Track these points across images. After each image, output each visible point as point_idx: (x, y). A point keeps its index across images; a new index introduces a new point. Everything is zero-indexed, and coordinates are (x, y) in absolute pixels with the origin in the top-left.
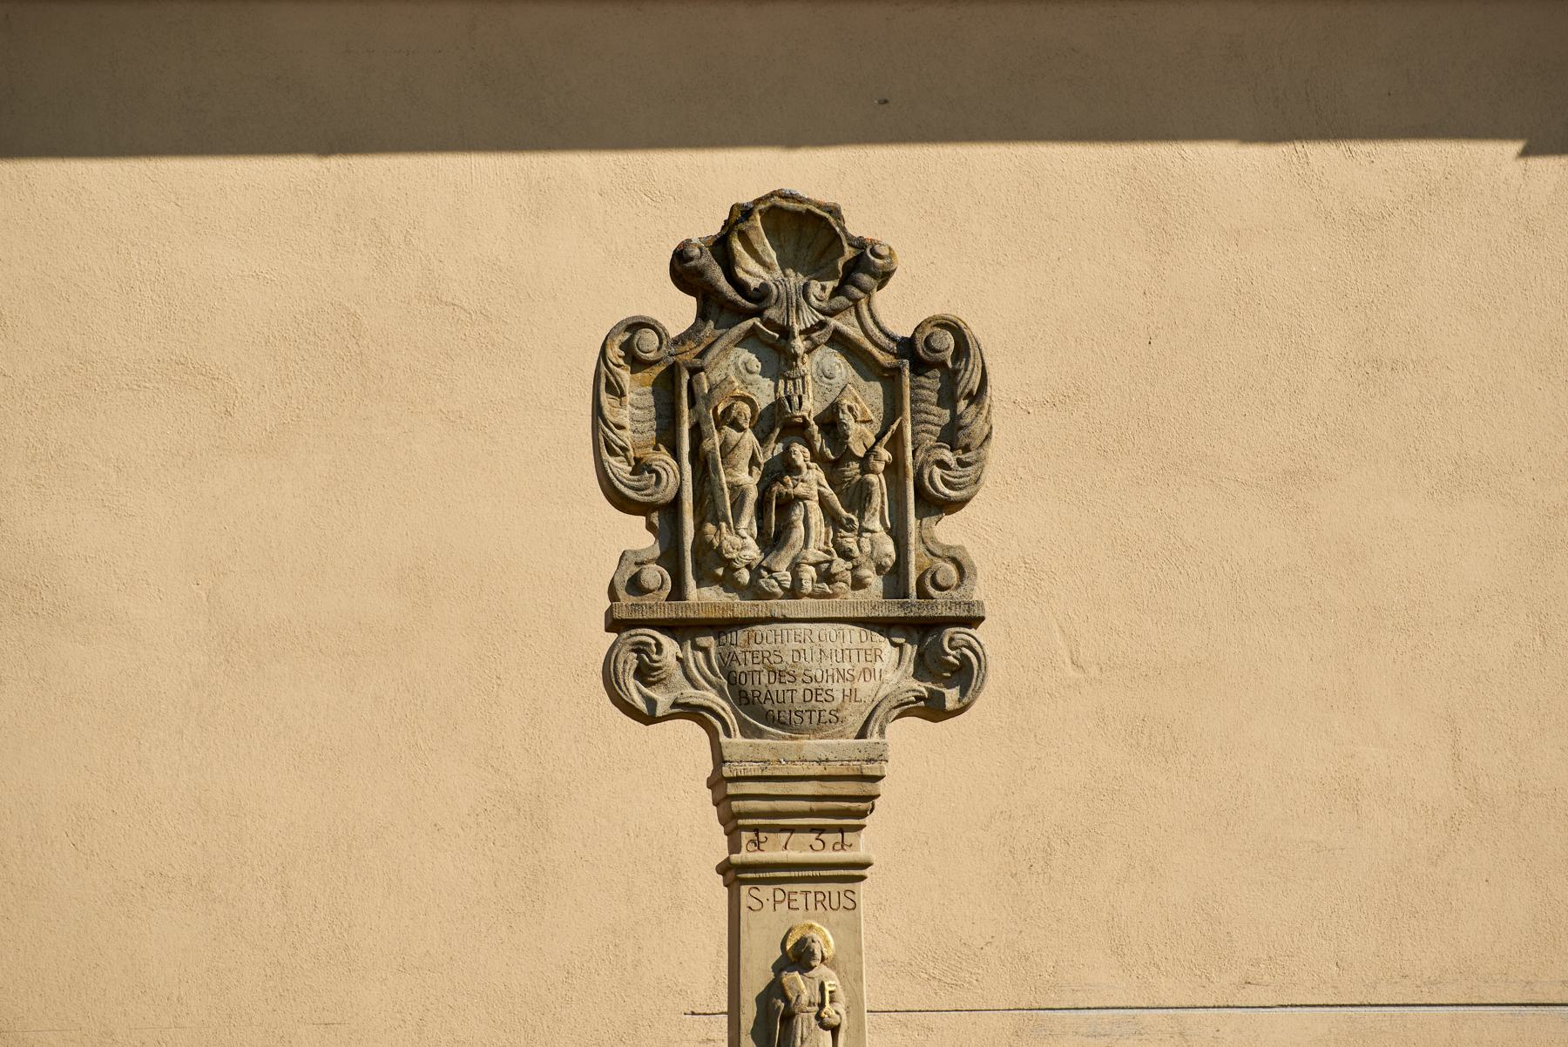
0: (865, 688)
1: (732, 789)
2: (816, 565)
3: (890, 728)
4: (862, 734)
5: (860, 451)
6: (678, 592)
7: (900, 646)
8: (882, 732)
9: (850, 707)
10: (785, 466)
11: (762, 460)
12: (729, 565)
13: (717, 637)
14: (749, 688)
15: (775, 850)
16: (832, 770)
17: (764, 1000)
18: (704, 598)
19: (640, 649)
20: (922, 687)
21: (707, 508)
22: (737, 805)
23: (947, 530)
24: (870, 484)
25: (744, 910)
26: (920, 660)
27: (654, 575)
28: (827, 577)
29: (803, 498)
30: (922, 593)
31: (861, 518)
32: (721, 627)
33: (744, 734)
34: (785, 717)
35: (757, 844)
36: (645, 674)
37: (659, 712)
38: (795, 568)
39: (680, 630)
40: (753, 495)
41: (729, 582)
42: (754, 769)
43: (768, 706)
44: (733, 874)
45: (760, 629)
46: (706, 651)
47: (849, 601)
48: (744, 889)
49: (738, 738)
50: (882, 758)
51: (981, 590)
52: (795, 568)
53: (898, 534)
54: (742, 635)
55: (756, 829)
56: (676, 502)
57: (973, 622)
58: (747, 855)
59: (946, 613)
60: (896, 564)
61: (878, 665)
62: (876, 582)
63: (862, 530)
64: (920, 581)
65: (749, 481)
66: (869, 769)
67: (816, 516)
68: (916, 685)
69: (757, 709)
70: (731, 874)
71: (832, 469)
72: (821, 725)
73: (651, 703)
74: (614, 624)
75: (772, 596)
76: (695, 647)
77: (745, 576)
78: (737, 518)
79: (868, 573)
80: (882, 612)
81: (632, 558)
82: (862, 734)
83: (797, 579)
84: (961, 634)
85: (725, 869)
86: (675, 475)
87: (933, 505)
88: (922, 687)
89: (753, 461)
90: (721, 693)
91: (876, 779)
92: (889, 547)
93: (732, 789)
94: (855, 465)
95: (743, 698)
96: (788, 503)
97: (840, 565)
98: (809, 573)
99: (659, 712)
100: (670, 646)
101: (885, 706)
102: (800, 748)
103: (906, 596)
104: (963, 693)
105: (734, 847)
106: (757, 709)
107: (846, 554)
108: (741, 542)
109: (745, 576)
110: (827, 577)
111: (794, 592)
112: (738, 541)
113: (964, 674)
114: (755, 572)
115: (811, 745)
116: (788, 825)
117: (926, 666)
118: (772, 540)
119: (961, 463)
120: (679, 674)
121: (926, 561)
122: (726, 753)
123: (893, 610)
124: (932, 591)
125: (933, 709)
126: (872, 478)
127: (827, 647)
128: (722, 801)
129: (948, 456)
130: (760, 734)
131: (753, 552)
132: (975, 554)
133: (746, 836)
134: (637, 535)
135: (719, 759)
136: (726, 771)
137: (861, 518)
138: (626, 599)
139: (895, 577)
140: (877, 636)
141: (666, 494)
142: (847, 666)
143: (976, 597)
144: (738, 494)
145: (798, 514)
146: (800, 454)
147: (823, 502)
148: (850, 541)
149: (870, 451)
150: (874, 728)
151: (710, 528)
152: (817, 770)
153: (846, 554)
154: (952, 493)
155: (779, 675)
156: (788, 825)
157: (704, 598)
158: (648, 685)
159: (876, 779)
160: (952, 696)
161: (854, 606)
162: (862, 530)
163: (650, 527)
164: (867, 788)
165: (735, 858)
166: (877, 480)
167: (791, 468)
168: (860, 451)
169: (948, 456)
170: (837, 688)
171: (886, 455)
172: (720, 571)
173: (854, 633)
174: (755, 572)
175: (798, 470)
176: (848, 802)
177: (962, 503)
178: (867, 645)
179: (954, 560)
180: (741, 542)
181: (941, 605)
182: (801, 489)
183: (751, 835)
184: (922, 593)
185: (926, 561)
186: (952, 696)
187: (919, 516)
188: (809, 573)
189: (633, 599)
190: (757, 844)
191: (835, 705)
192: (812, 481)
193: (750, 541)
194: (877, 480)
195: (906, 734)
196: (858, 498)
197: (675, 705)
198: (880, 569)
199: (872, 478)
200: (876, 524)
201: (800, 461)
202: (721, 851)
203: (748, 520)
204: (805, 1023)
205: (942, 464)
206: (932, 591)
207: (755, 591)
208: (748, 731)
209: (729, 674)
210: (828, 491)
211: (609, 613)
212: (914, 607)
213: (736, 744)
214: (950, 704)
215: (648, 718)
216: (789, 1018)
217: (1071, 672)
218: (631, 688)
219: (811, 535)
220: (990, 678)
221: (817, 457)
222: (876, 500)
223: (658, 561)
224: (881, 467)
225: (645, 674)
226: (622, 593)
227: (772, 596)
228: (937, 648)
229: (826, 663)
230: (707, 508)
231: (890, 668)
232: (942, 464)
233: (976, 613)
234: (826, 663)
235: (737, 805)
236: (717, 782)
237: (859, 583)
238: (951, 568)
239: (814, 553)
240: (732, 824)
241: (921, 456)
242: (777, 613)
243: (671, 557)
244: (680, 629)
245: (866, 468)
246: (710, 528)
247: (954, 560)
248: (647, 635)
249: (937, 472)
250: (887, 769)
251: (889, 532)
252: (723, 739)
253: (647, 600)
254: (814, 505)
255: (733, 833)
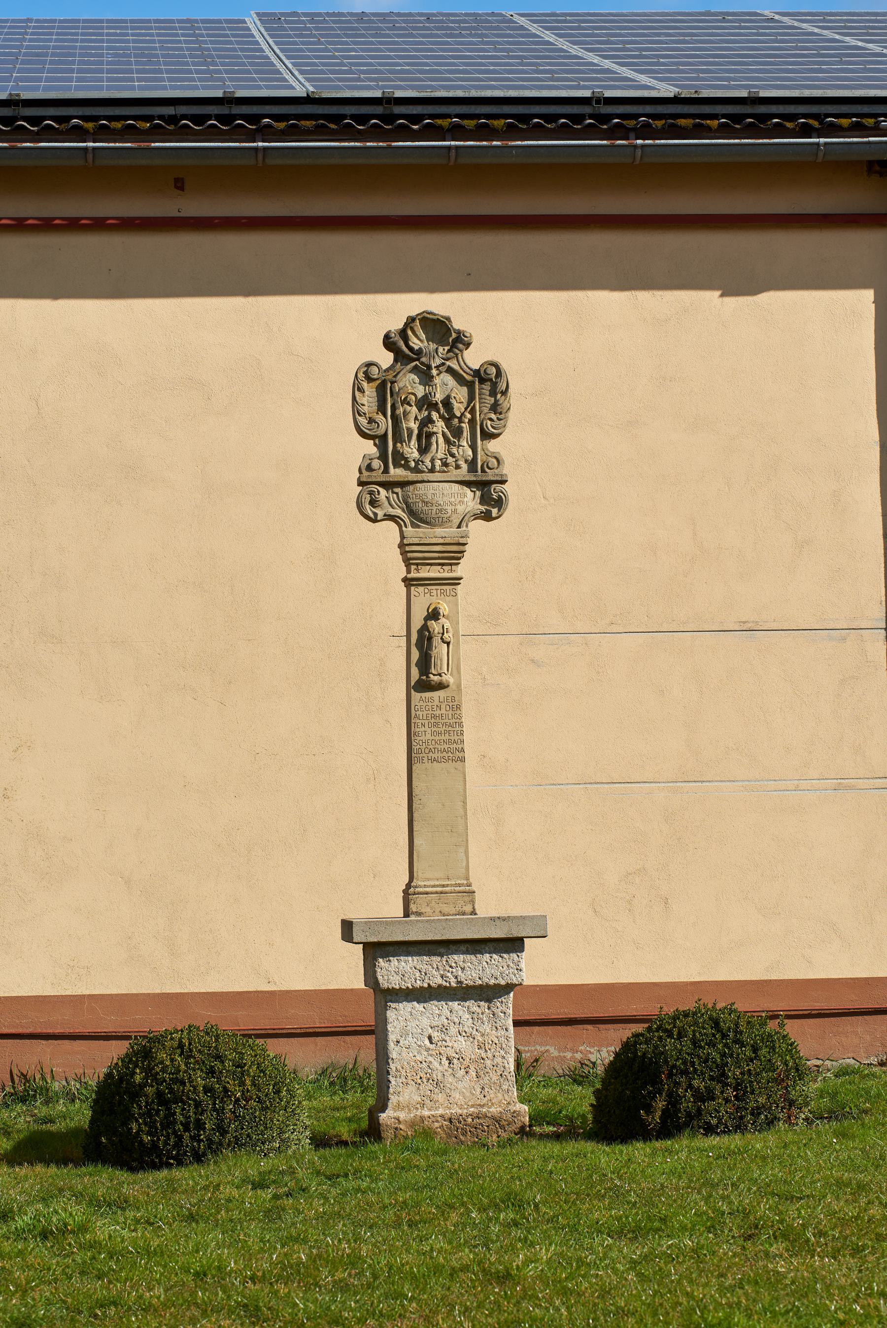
0: (461, 509)
1: (407, 549)
2: (441, 460)
3: (470, 524)
4: (459, 527)
5: (458, 415)
6: (386, 471)
7: (474, 492)
8: (467, 526)
9: (454, 516)
10: (429, 420)
11: (419, 418)
12: (406, 460)
13: (402, 488)
14: (414, 508)
16: (447, 541)
17: (420, 632)
18: (397, 473)
19: (371, 493)
20: (483, 508)
21: (398, 438)
23: (493, 446)
24: (462, 427)
25: (412, 596)
26: (482, 495)
27: (377, 464)
28: (445, 464)
29: (436, 433)
30: (483, 471)
31: (459, 441)
32: (403, 484)
33: (412, 527)
34: (428, 520)
35: (418, 570)
36: (373, 503)
37: (379, 518)
38: (432, 461)
39: (387, 485)
40: (416, 432)
41: (406, 467)
42: (416, 541)
43: (422, 516)
44: (408, 582)
45: (418, 485)
46: (397, 494)
47: (455, 474)
48: (413, 588)
49: (410, 528)
50: (467, 536)
51: (507, 470)
52: (432, 461)
53: (473, 447)
54: (411, 487)
55: (417, 564)
56: (386, 434)
57: (503, 482)
58: (413, 575)
59: (492, 479)
60: (473, 459)
61: (466, 499)
62: (465, 467)
63: (459, 446)
64: (482, 466)
65: (414, 426)
66: (462, 541)
67: (441, 440)
69: (417, 517)
70: (407, 582)
71: (448, 421)
73: (376, 514)
74: (361, 483)
76: (393, 492)
77: (413, 464)
78: (409, 441)
79: (462, 463)
80: (467, 478)
81: (368, 457)
82: (459, 527)
83: (433, 465)
84: (498, 487)
85: (405, 580)
86: (385, 424)
87: (488, 436)
88: (483, 508)
90: (403, 511)
91: (465, 544)
92: (470, 452)
93: (407, 549)
94: (456, 420)
95: (412, 512)
96: (430, 435)
97: (450, 460)
98: (438, 463)
99: (379, 518)
100: (383, 492)
101: (468, 515)
102: (435, 532)
103: (477, 472)
104: (499, 510)
105: (409, 572)
106: (417, 517)
107: (453, 456)
108: (411, 451)
109: (413, 464)
110: (445, 464)
111: (432, 470)
112: (410, 450)
113: (499, 503)
114: (417, 463)
115: (439, 531)
116: (430, 563)
117: (484, 500)
118: (423, 450)
119: (499, 419)
120: (386, 503)
121: (485, 458)
124: (487, 470)
125: (487, 517)
126: (463, 425)
128: (404, 553)
129: (493, 416)
130: (419, 527)
131: (416, 455)
132: (504, 455)
133: (413, 567)
134: (370, 448)
135: (402, 537)
136: (405, 542)
137: (459, 441)
138: (365, 473)
139: (472, 465)
140: (465, 488)
141: (381, 431)
142: (453, 500)
143: (504, 472)
144: (410, 432)
145: (434, 439)
146: (435, 415)
147: (444, 434)
149: (462, 414)
150: (464, 524)
151: (399, 445)
152: (441, 541)
153: (453, 456)
154: (495, 431)
155: (426, 503)
156: (430, 563)
157: (397, 473)
158: (374, 507)
159: (465, 544)
162: (459, 446)
163: (375, 444)
164: (461, 548)
165: (409, 576)
166: (465, 426)
167: (432, 421)
168: (458, 415)
169: (493, 416)
170: (449, 509)
171: (469, 416)
172: (403, 462)
173: (456, 487)
174: (417, 463)
175: (434, 422)
176: (453, 554)
177: (498, 435)
178: (461, 491)
179: (496, 458)
180: (411, 451)
181: (490, 475)
182: (435, 430)
183: (415, 567)
184: (483, 471)
186: (495, 512)
187: (482, 440)
188: (438, 463)
189: (368, 473)
190: (418, 570)
191: (448, 515)
192: (439, 426)
193: (415, 450)
194: (465, 426)
195: (477, 527)
196: (457, 433)
197: (385, 515)
198: (466, 461)
199: (463, 425)
200: (465, 444)
201: (435, 418)
202: (403, 573)
203: (414, 442)
204: (436, 641)
205: (491, 420)
206: (487, 470)
207: (417, 470)
208: (414, 525)
209: (406, 503)
210: (446, 430)
211: (359, 479)
213: (409, 530)
214: (494, 515)
215: (374, 520)
216: (430, 639)
217: (543, 500)
218: (368, 509)
219: (439, 448)
220: (509, 506)
221: (442, 417)
222: (465, 434)
223: (378, 458)
224: (467, 420)
225: (373, 503)
226: (364, 471)
227: (423, 472)
229: (445, 499)
230: (398, 437)
231: (470, 500)
232: (491, 420)
233: (504, 478)
236: (401, 546)
237: (458, 467)
238: (495, 461)
239: (440, 455)
240: (408, 563)
242: (425, 479)
243: (383, 457)
244: (387, 485)
245: (461, 421)
246: (399, 445)
247: (496, 458)
249: (489, 422)
250: (469, 541)
251: (470, 446)
252: (404, 528)
253: (374, 474)
254: (440, 436)
255: (408, 566)
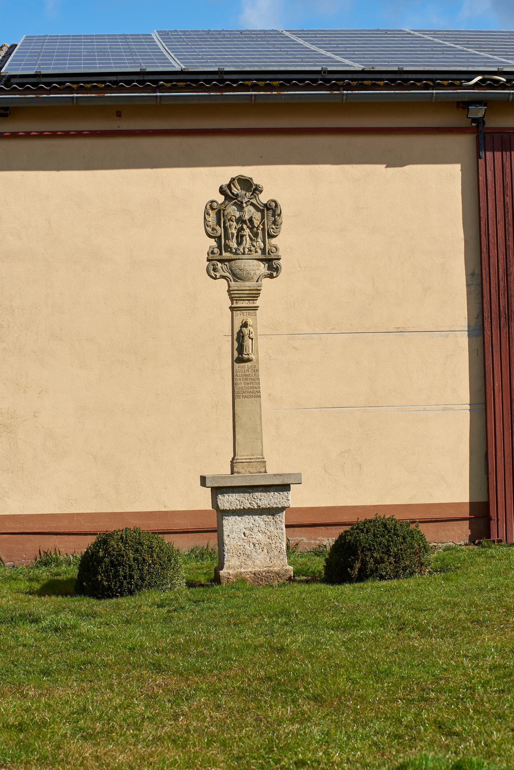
0: (258, 272)
1: (232, 292)
3: (262, 280)
4: (257, 281)
5: (256, 226)
6: (221, 254)
9: (255, 276)
12: (231, 248)
14: (235, 272)
15: (240, 304)
16: (251, 288)
17: (238, 333)
18: (226, 255)
19: (213, 265)
20: (269, 272)
21: (227, 237)
22: (233, 295)
23: (274, 241)
26: (268, 266)
27: (216, 250)
28: (250, 250)
30: (269, 254)
32: (229, 260)
34: (242, 278)
35: (237, 303)
36: (215, 270)
38: (244, 249)
39: (222, 260)
40: (235, 235)
41: (231, 252)
44: (232, 309)
46: (226, 265)
48: (234, 312)
49: (233, 282)
51: (280, 253)
52: (244, 249)
53: (264, 242)
54: (233, 262)
55: (237, 300)
56: (221, 236)
57: (279, 259)
58: (235, 305)
59: (273, 257)
62: (260, 252)
63: (257, 241)
64: (268, 251)
65: (235, 232)
66: (259, 288)
67: (248, 238)
68: (268, 272)
69: (237, 277)
71: (251, 229)
72: (249, 279)
73: (216, 275)
74: (208, 260)
75: (239, 254)
76: (224, 265)
77: (234, 251)
78: (232, 239)
79: (258, 250)
80: (261, 257)
82: (257, 281)
84: (276, 262)
86: (220, 231)
87: (271, 236)
88: (269, 272)
89: (236, 228)
90: (230, 273)
92: (262, 245)
93: (232, 292)
94: (255, 229)
95: (234, 274)
96: (242, 236)
97: (253, 248)
98: (247, 250)
100: (219, 265)
104: (277, 273)
105: (232, 304)
106: (237, 277)
107: (254, 246)
108: (233, 244)
109: (234, 251)
110: (250, 250)
111: (244, 254)
113: (277, 269)
114: (236, 250)
115: (247, 284)
116: (243, 300)
117: (270, 268)
118: (239, 243)
120: (221, 270)
121: (270, 247)
122: (231, 285)
123: (263, 257)
125: (271, 276)
127: (250, 264)
128: (230, 295)
129: (274, 227)
130: (237, 281)
131: (236, 246)
133: (235, 302)
134: (213, 243)
135: (229, 286)
136: (231, 289)
138: (211, 255)
139: (263, 251)
141: (218, 234)
144: (233, 234)
145: (244, 238)
146: (245, 226)
147: (249, 236)
148: (255, 244)
149: (258, 226)
150: (260, 280)
151: (227, 241)
152: (248, 288)
153: (254, 246)
155: (241, 270)
156: (243, 300)
157: (226, 255)
160: (275, 274)
161: (255, 256)
162: (257, 241)
163: (215, 241)
164: (258, 292)
165: (233, 306)
166: (260, 232)
167: (243, 230)
168: (256, 226)
169: (274, 227)
170: (252, 272)
171: (262, 227)
174: (236, 250)
175: (244, 230)
176: (255, 295)
177: (276, 236)
179: (275, 247)
180: (233, 244)
181: (273, 256)
182: (245, 233)
184: (269, 254)
185: (270, 247)
186: (275, 274)
187: (268, 239)
188: (247, 250)
189: (212, 255)
190: (237, 303)
192: (247, 232)
193: (235, 244)
194: (260, 232)
195: (266, 281)
196: (256, 235)
198: (260, 249)
200: (260, 240)
202: (230, 304)
203: (234, 239)
204: (246, 338)
205: (273, 228)
207: (236, 254)
208: (235, 281)
210: (250, 234)
211: (207, 258)
212: (267, 256)
213: (232, 283)
214: (274, 276)
215: (215, 278)
216: (243, 337)
217: (299, 268)
218: (212, 273)
219: (247, 243)
221: (248, 227)
222: (260, 235)
225: (215, 270)
226: (210, 254)
227: (239, 254)
228: (272, 265)
229: (250, 268)
230: (227, 237)
231: (263, 268)
232: (273, 228)
233: (279, 257)
234: (250, 268)
235: (233, 295)
236: (229, 291)
237: (256, 252)
238: (275, 249)
239: (248, 246)
240: (232, 299)
241: (268, 227)
243: (219, 247)
244: (222, 261)
245: (258, 229)
246: (227, 241)
247: (275, 247)
248: (215, 262)
249: (272, 230)
253: (215, 255)
254: (247, 236)
255: (232, 301)
